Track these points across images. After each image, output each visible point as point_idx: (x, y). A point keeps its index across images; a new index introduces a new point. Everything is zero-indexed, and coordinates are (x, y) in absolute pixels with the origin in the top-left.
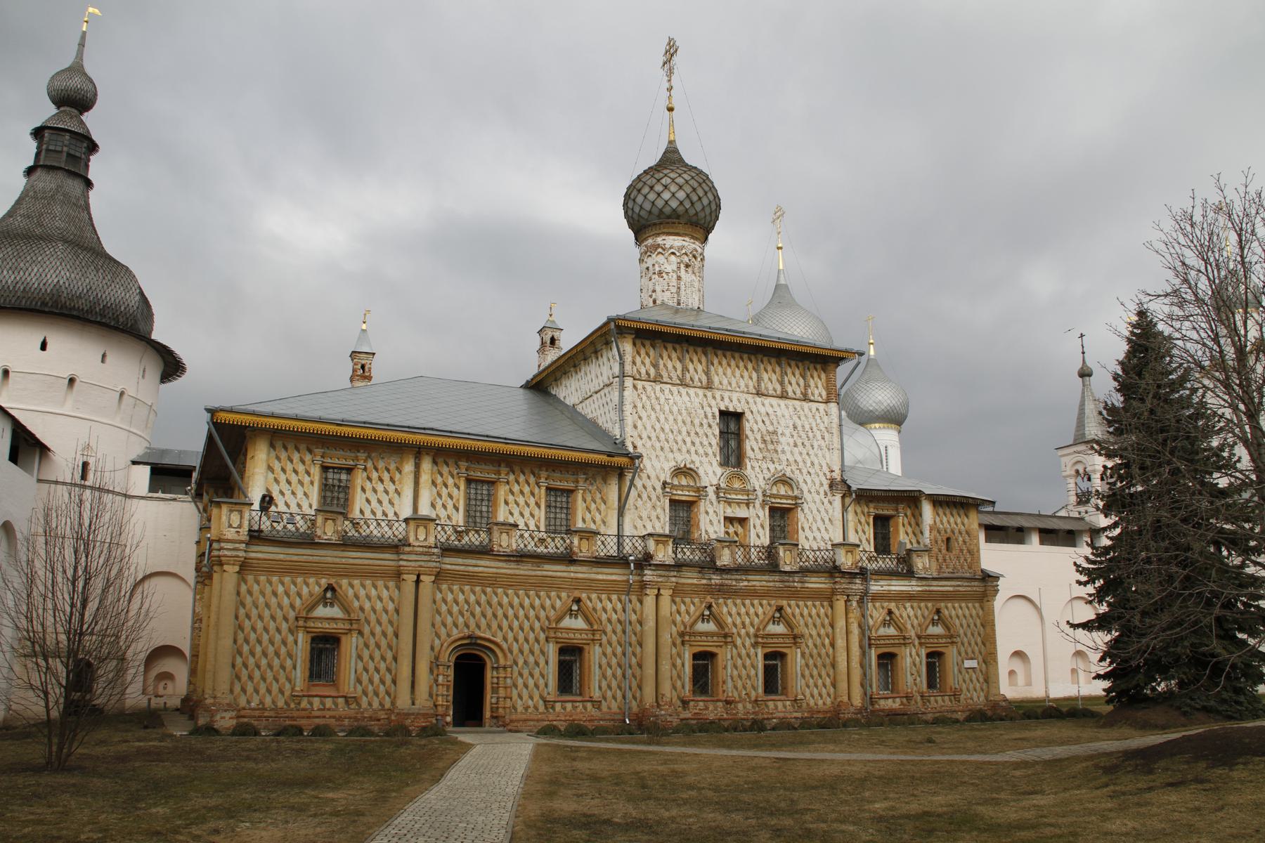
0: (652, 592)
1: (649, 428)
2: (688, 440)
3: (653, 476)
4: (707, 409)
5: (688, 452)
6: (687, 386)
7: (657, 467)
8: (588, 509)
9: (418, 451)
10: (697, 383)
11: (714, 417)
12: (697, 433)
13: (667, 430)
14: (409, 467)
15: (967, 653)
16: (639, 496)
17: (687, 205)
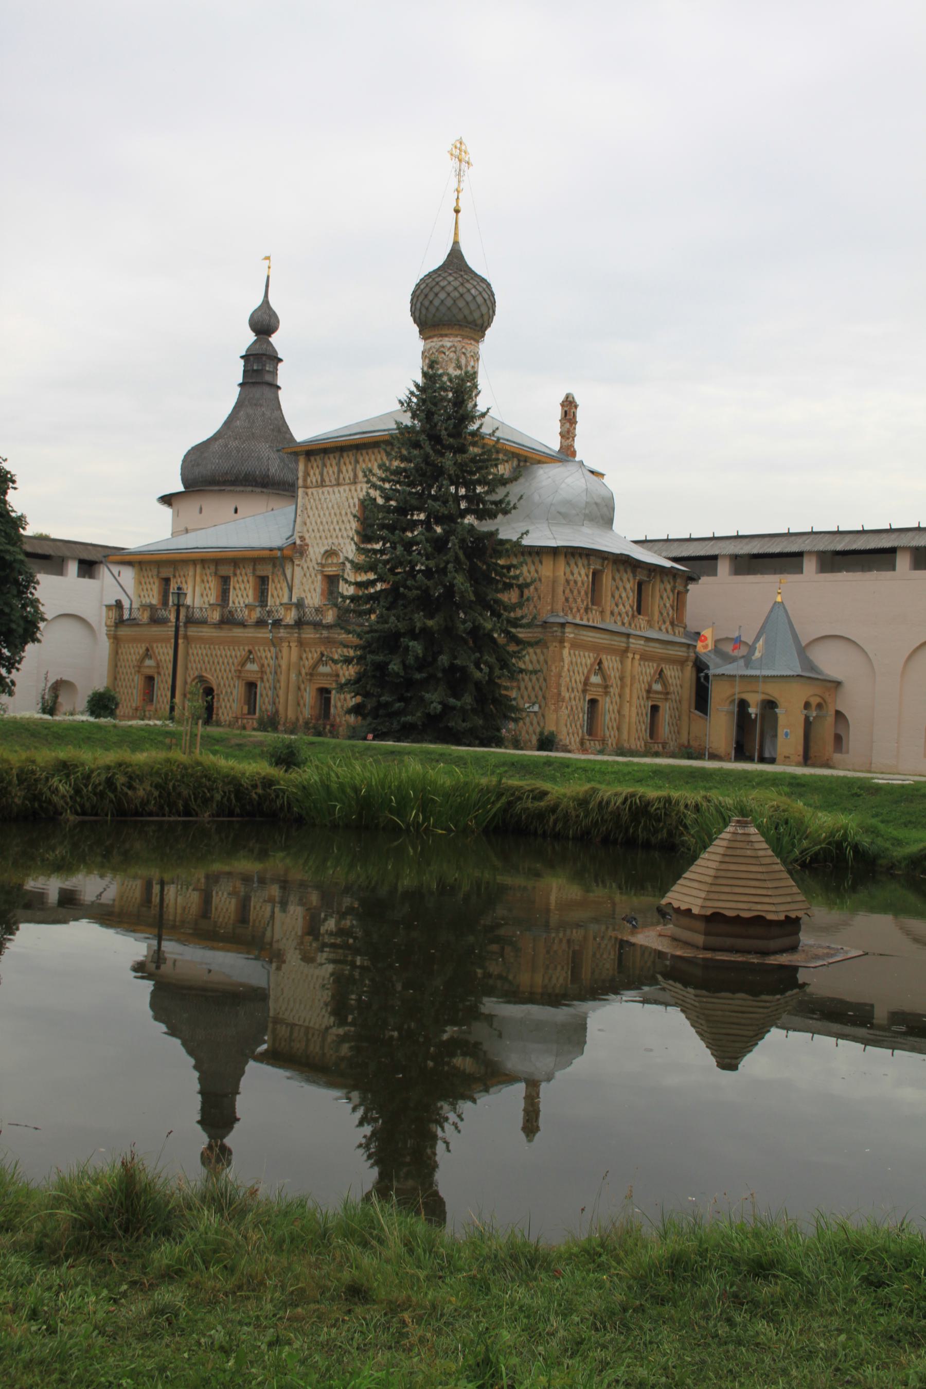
0: (285, 644)
1: (314, 523)
2: (337, 528)
3: (314, 559)
4: (351, 501)
5: (337, 537)
6: (338, 484)
7: (315, 552)
8: (276, 589)
9: (194, 562)
10: (347, 481)
11: (355, 506)
12: (343, 521)
13: (324, 523)
14: (191, 573)
15: (529, 697)
16: (305, 575)
17: (424, 311)
